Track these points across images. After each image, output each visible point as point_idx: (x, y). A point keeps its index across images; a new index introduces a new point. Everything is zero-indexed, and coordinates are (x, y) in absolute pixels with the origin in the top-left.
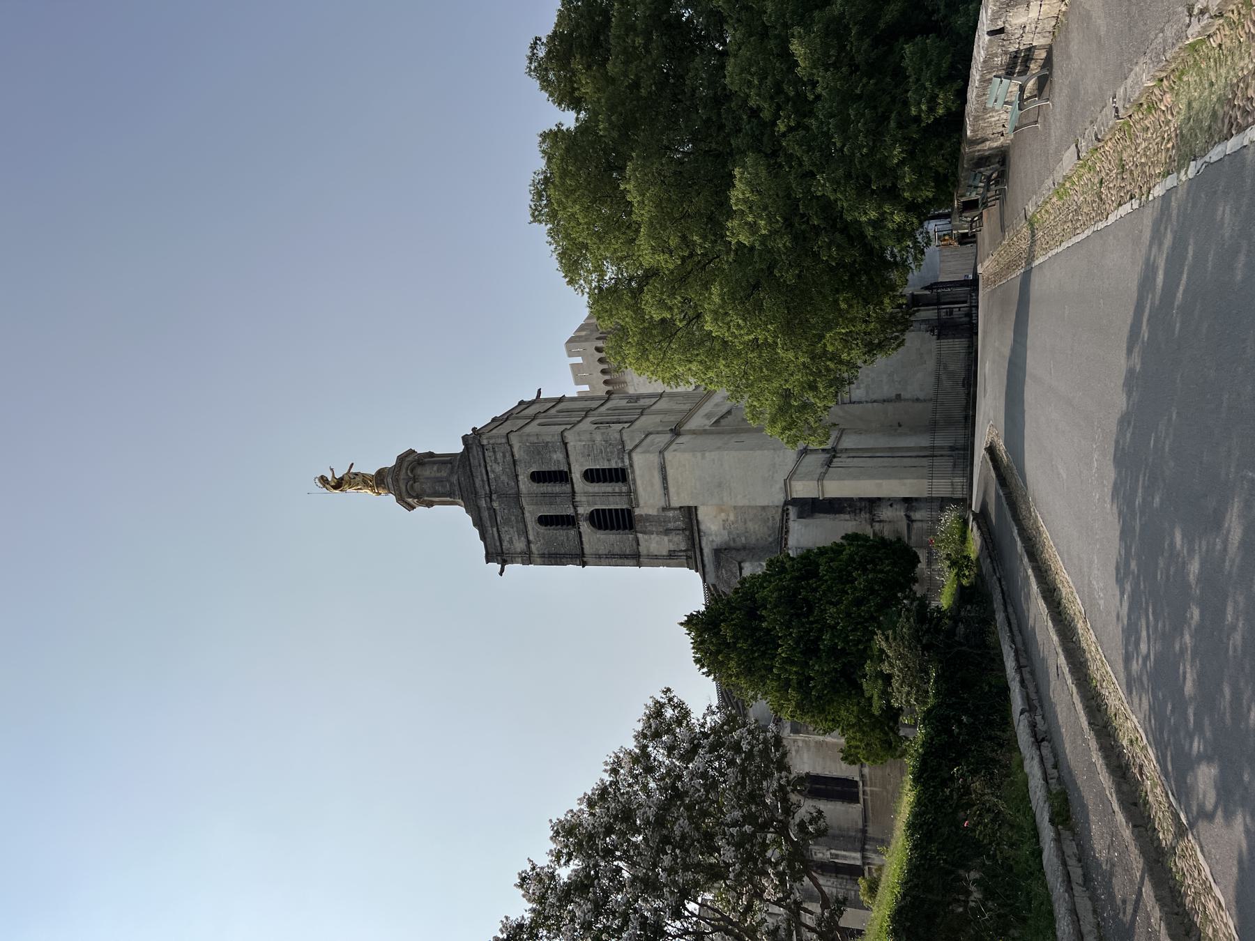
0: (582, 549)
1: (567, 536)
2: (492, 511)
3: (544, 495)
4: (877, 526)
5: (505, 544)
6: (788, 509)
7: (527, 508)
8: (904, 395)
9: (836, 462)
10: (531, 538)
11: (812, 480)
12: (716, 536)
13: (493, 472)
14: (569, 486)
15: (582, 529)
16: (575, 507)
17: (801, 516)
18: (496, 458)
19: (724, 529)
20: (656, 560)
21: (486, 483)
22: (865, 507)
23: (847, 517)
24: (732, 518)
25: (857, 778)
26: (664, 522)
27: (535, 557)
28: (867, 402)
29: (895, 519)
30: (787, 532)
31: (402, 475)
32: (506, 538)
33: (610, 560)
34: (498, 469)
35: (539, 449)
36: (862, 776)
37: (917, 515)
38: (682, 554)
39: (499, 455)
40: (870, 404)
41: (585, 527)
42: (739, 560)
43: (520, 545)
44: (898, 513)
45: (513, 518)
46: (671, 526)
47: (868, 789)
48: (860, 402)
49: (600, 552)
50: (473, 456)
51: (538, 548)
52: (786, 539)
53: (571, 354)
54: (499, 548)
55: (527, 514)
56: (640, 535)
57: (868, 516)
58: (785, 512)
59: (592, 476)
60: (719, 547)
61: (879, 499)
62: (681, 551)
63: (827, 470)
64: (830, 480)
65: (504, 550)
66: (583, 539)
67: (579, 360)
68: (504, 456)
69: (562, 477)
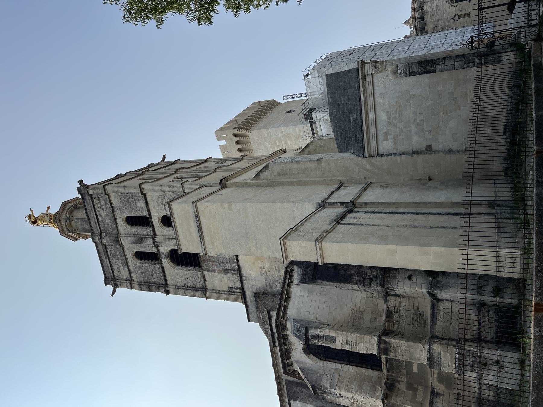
0: (166, 280)
2: (104, 246)
3: (136, 235)
4: (392, 302)
5: (116, 273)
6: (292, 270)
7: (127, 246)
8: (435, 147)
9: (350, 218)
11: (309, 240)
12: (255, 280)
13: (101, 216)
16: (157, 247)
17: (303, 281)
18: (101, 205)
19: (262, 275)
20: (219, 294)
22: (377, 277)
23: (355, 287)
24: (267, 266)
26: (223, 262)
27: (135, 284)
28: (395, 154)
29: (416, 295)
30: (288, 299)
31: (63, 216)
32: (115, 267)
33: (185, 291)
35: (127, 199)
37: (444, 295)
38: (238, 291)
39: (103, 203)
40: (398, 158)
41: (166, 263)
42: (269, 308)
44: (418, 290)
45: (118, 252)
46: (228, 266)
48: (388, 155)
49: (179, 284)
50: (87, 203)
51: (136, 277)
52: (286, 308)
53: (219, 139)
55: (126, 251)
56: (206, 273)
57: (380, 288)
58: (289, 273)
60: (258, 291)
61: (395, 269)
62: (237, 288)
63: (334, 228)
64: (326, 242)
65: (116, 277)
66: (166, 273)
67: (224, 142)
68: (106, 204)
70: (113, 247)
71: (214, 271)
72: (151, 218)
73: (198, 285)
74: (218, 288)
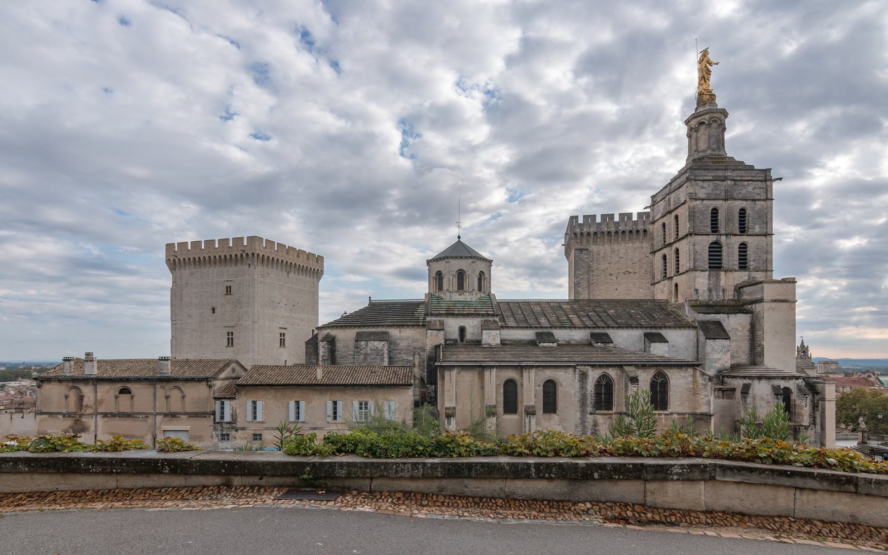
1: (707, 226)
13: (748, 185)
14: (738, 233)
15: (711, 237)
21: (741, 179)
25: (669, 411)
34: (750, 189)
36: (672, 414)
39: (758, 191)
41: (713, 238)
47: (663, 416)
49: (696, 246)
50: (758, 173)
55: (720, 202)
56: (707, 273)
59: (743, 247)
68: (758, 194)
69: (743, 230)
70: (723, 188)
71: (709, 280)
72: (748, 235)
73: (697, 264)
74: (696, 281)
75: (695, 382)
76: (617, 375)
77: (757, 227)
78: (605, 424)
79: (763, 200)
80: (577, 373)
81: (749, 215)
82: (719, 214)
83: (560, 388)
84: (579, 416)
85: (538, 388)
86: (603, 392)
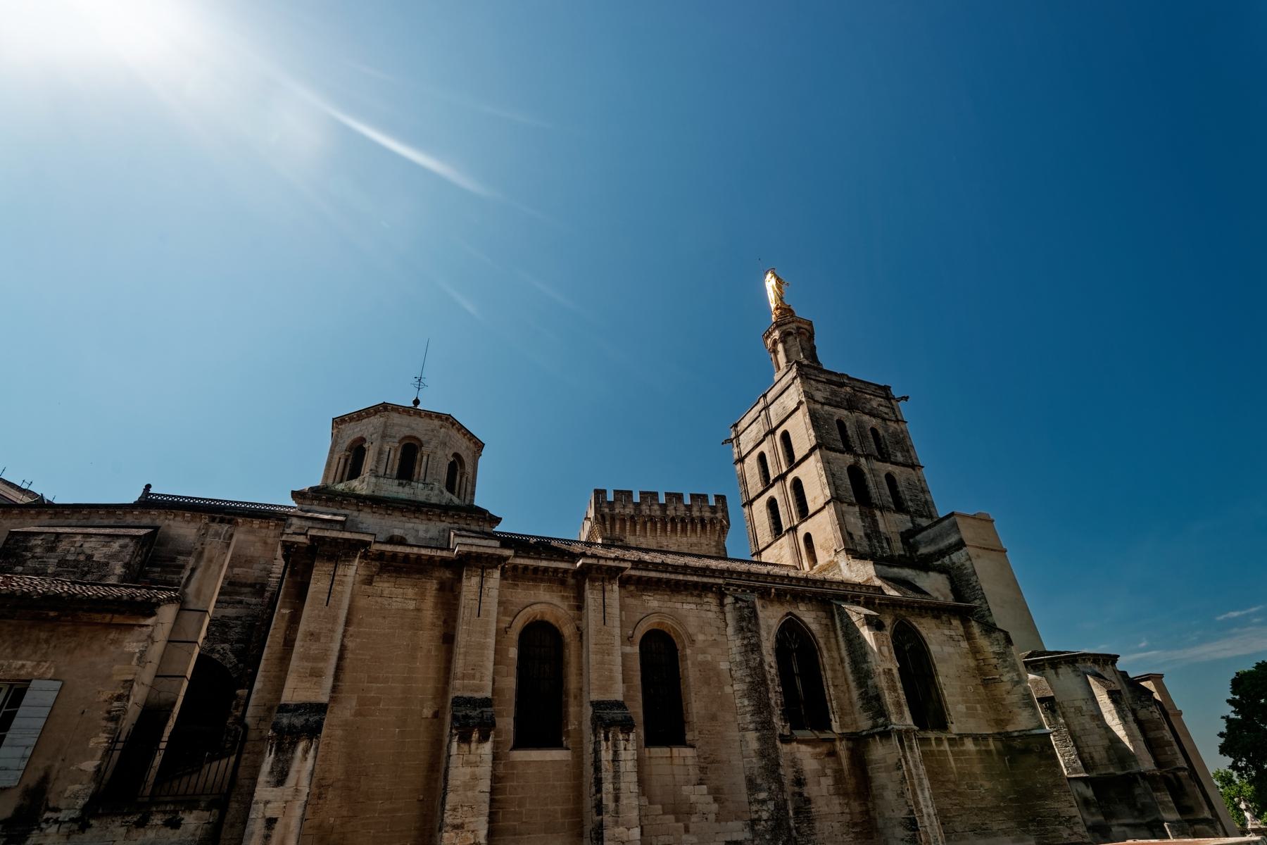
1: (837, 440)
5: (813, 382)
10: (826, 408)
18: (882, 406)
32: (820, 386)
34: (875, 404)
36: (962, 736)
39: (886, 410)
41: (849, 459)
43: (819, 396)
45: (839, 399)
54: (810, 377)
55: (845, 412)
59: (890, 478)
68: (886, 413)
75: (975, 651)
76: (821, 624)
77: (899, 454)
78: (825, 775)
79: (895, 422)
80: (728, 608)
81: (883, 436)
82: (848, 429)
83: (688, 651)
84: (755, 745)
85: (628, 649)
86: (796, 669)
